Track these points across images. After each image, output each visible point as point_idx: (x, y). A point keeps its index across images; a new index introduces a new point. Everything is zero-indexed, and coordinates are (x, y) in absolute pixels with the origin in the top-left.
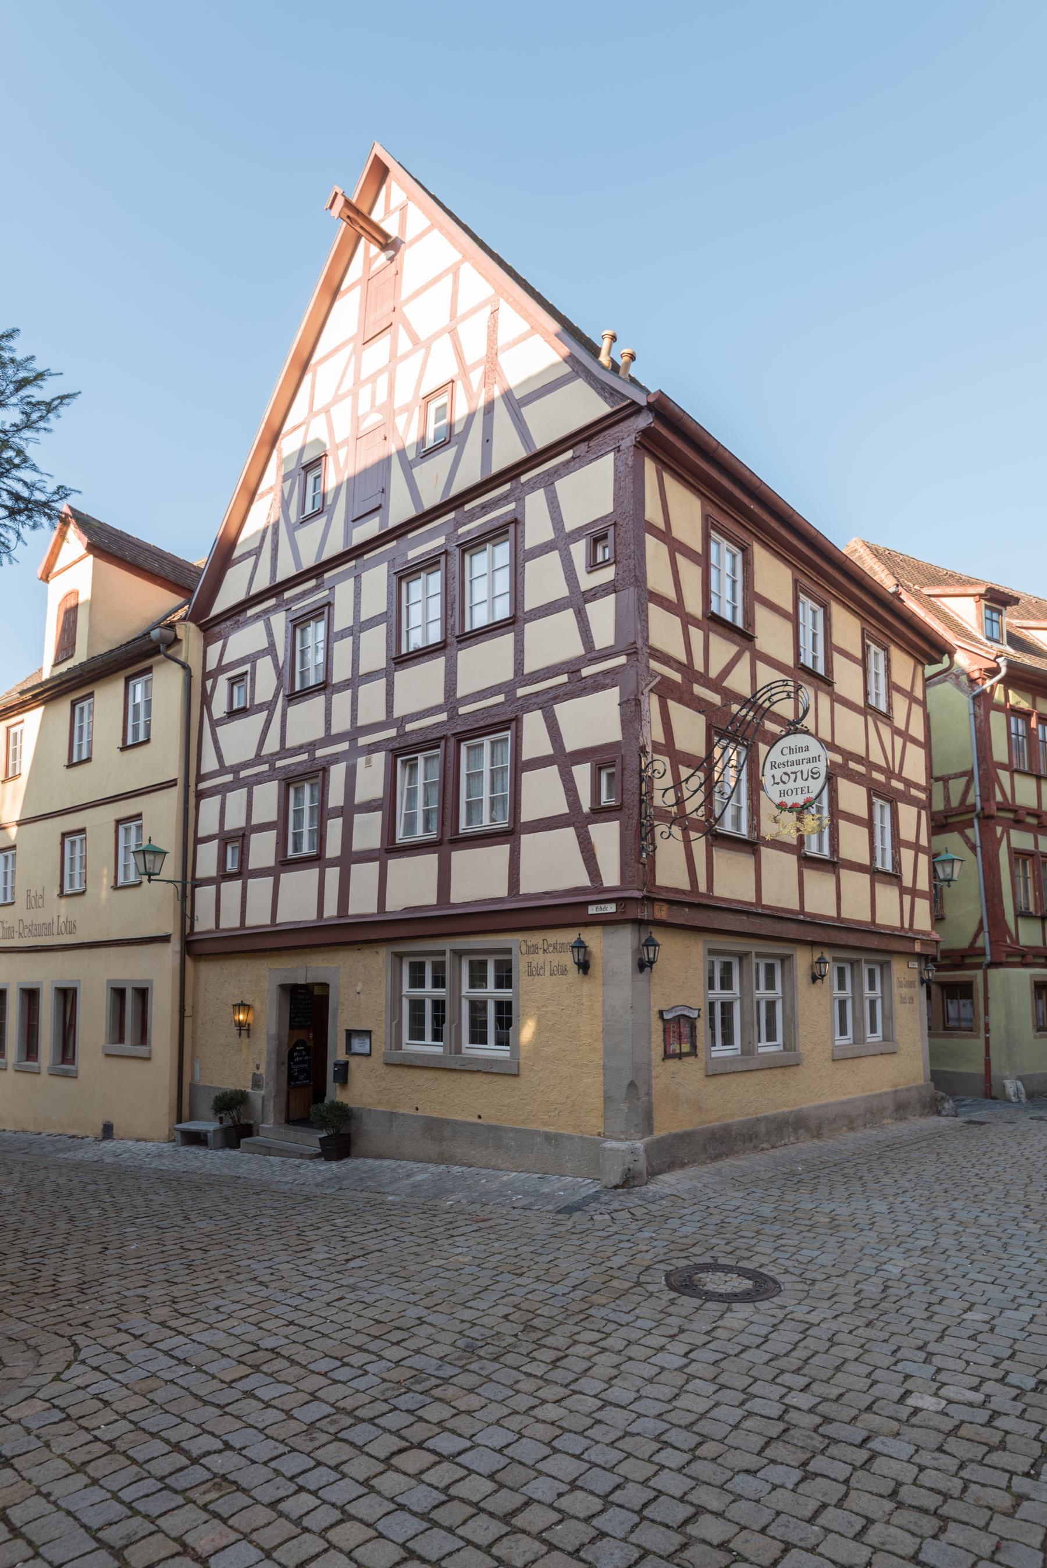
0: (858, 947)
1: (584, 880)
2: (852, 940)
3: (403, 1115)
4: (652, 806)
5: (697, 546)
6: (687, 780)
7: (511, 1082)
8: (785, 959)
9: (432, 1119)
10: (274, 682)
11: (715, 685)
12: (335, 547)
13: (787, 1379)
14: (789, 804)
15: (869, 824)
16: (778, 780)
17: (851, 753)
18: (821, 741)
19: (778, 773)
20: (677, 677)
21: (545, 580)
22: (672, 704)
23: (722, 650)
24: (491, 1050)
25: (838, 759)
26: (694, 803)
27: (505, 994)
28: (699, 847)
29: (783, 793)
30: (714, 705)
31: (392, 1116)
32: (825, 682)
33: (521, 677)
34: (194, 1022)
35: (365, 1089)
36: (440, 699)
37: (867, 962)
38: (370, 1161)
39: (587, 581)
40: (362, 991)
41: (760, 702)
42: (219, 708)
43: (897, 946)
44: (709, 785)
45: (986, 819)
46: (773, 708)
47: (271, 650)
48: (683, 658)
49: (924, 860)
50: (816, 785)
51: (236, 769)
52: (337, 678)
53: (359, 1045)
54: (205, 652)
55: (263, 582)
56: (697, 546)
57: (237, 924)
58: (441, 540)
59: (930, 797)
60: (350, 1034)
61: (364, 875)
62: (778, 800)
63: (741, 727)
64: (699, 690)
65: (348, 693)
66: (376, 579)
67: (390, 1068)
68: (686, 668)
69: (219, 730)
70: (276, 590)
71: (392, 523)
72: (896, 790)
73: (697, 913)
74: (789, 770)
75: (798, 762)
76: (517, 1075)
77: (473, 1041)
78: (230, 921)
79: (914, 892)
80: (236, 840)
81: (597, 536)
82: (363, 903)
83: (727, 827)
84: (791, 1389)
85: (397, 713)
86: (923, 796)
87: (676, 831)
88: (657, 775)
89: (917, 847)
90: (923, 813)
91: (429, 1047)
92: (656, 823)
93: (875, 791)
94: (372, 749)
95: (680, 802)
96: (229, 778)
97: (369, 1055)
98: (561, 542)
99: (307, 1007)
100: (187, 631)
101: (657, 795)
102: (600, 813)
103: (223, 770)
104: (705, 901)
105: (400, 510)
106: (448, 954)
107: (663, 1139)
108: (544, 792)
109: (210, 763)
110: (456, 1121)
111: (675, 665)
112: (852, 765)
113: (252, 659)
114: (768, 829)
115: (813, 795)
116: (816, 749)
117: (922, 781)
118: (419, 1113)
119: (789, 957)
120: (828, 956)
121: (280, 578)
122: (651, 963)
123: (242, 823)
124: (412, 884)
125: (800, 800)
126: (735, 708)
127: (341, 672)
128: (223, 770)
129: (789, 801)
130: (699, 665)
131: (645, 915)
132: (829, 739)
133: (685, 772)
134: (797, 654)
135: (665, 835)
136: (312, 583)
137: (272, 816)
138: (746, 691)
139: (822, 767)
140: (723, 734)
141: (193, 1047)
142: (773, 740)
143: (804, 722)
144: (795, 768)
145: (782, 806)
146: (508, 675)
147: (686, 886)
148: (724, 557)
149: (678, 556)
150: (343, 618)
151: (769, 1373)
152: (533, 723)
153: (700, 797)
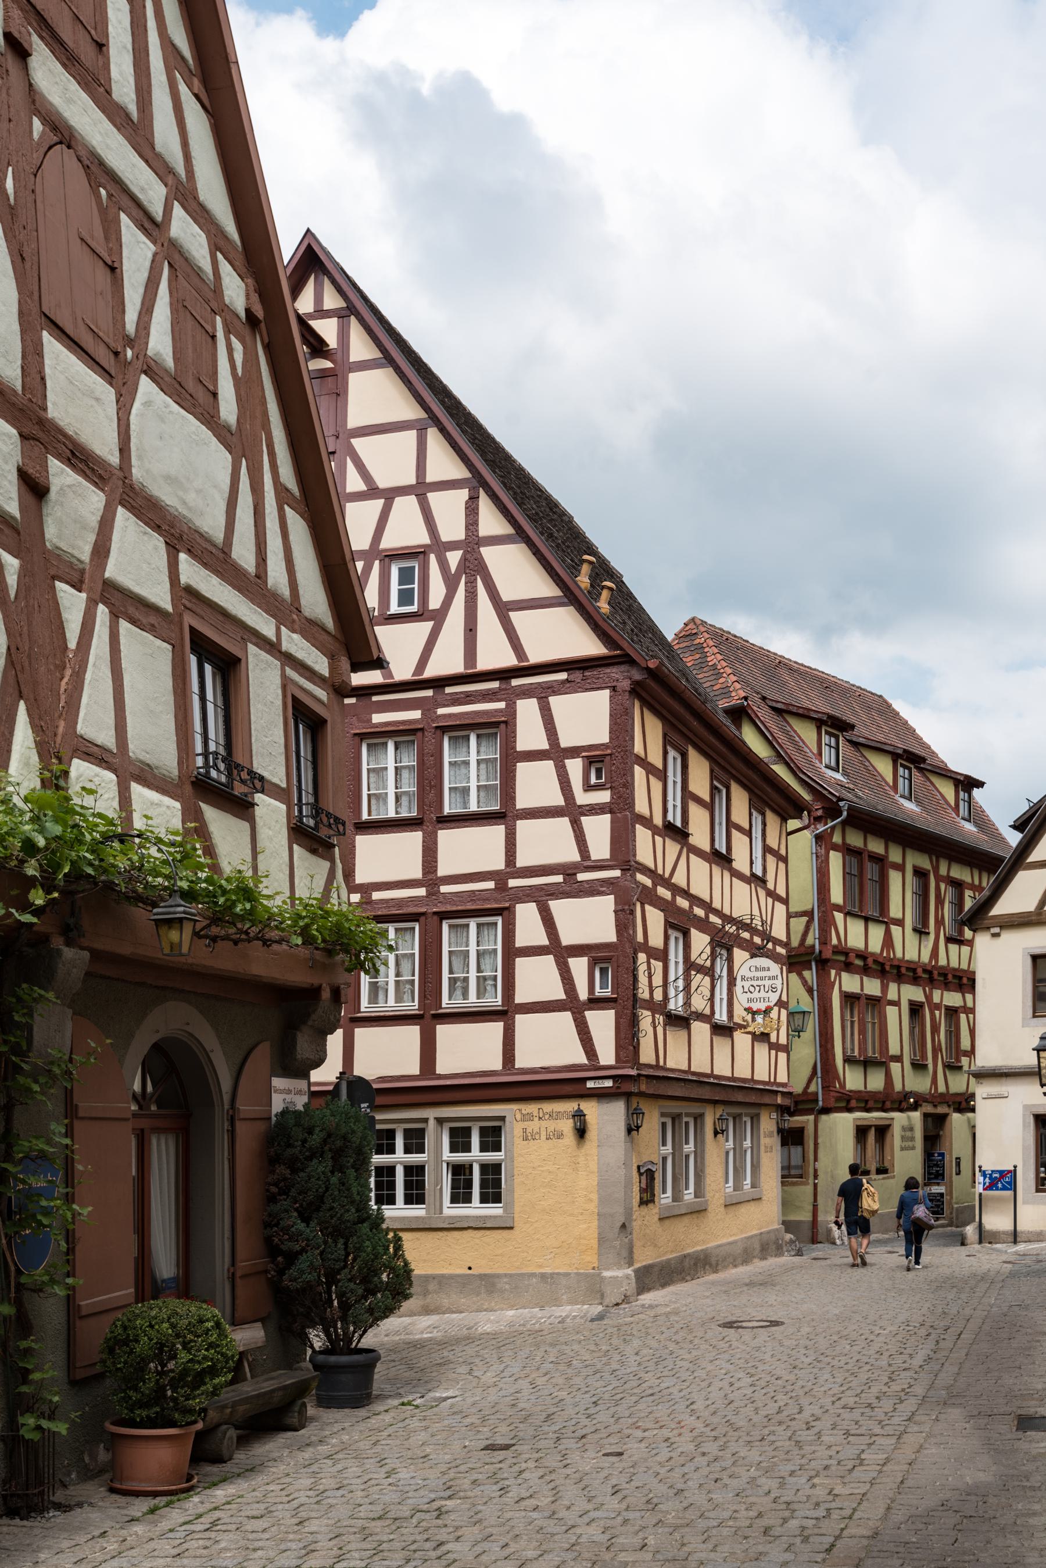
1: (582, 1059)
76: (511, 1228)
77: (455, 1199)
102: (596, 1003)
152: (527, 915)
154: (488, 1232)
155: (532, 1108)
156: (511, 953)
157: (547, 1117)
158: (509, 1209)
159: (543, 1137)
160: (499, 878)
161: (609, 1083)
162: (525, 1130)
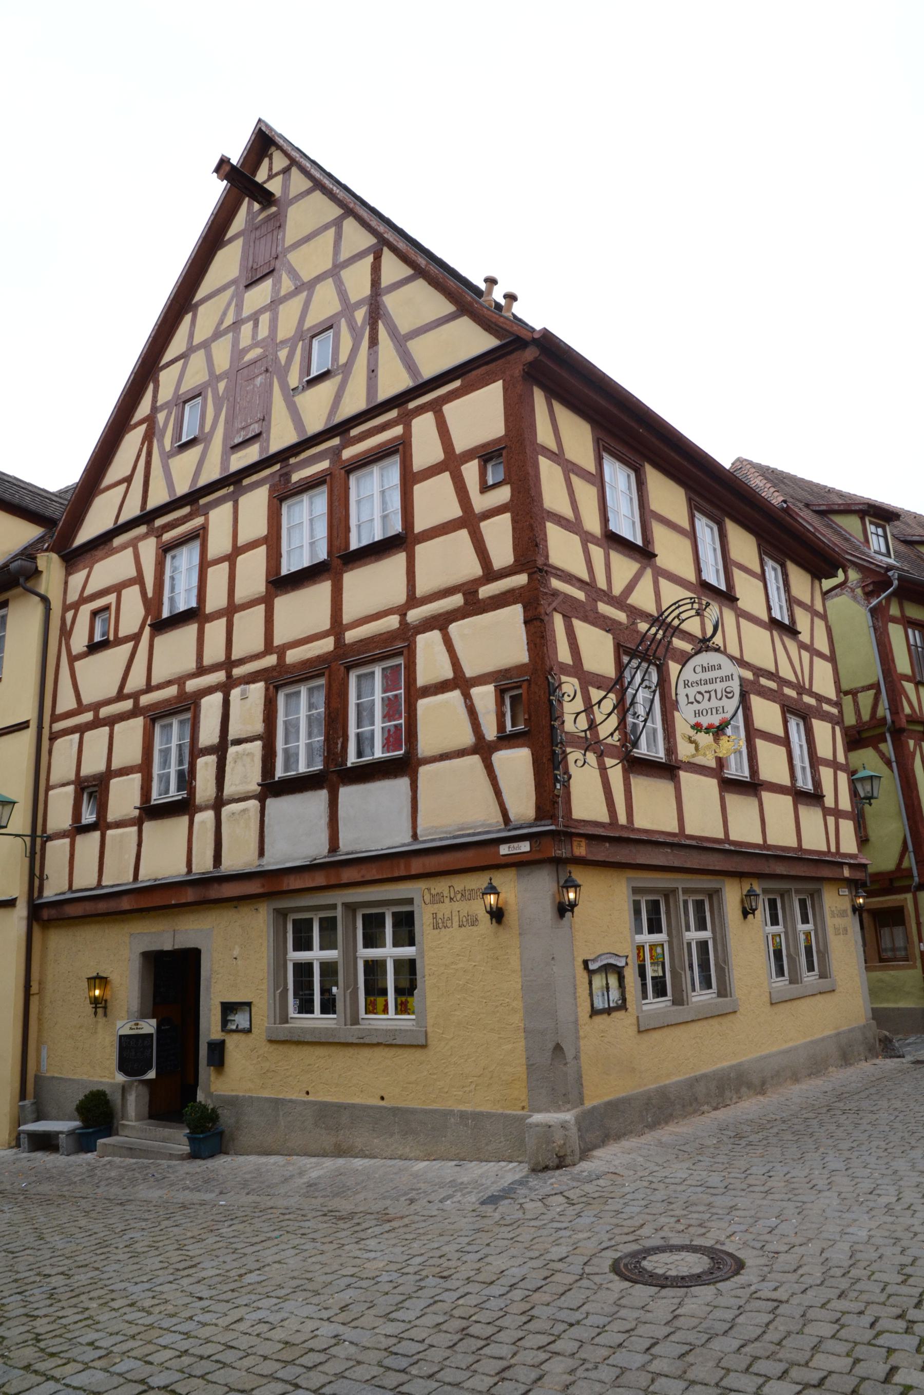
0: (783, 877)
2: (780, 869)
3: (291, 1101)
4: (563, 731)
6: (599, 703)
8: (714, 894)
10: (142, 612)
11: (619, 602)
12: (211, 474)
13: (761, 1367)
14: (705, 725)
15: (786, 742)
17: (760, 669)
18: (731, 658)
19: (691, 692)
20: (580, 595)
21: (436, 501)
22: (576, 623)
23: (624, 568)
24: (389, 1020)
25: (749, 675)
27: (407, 952)
28: (616, 774)
29: (698, 713)
30: (620, 623)
31: (277, 1103)
32: (728, 597)
33: (413, 601)
34: (41, 1001)
35: (243, 1074)
36: (326, 625)
37: (798, 891)
38: (253, 1158)
39: (480, 502)
40: (238, 959)
41: (669, 619)
43: (826, 872)
44: (623, 708)
45: (898, 734)
46: (682, 626)
47: (139, 580)
48: (585, 576)
49: (843, 777)
50: (731, 704)
51: (96, 707)
52: (210, 608)
55: (132, 510)
56: (591, 467)
57: (93, 882)
58: (325, 465)
59: (841, 712)
61: (240, 821)
62: (693, 721)
63: (648, 647)
64: (604, 608)
65: (223, 621)
66: (255, 503)
67: (275, 1046)
68: (588, 586)
69: (77, 664)
70: (147, 518)
71: (274, 448)
72: (809, 706)
73: (618, 848)
74: (703, 689)
75: (712, 681)
78: (86, 878)
79: (837, 813)
80: (93, 789)
82: (239, 856)
83: (643, 750)
84: (768, 1378)
85: (277, 642)
86: (835, 711)
87: (591, 757)
88: (566, 698)
89: (834, 764)
90: (837, 729)
91: (317, 1020)
92: (569, 750)
93: (789, 709)
94: (251, 678)
97: (249, 1031)
98: (451, 463)
99: (174, 979)
100: (49, 561)
101: (568, 719)
102: (506, 740)
105: (282, 435)
106: (339, 908)
107: (594, 1108)
108: (442, 722)
110: (353, 1106)
111: (577, 584)
112: (763, 681)
114: (684, 751)
115: (728, 716)
116: (729, 668)
117: (833, 696)
118: (311, 1098)
119: (718, 891)
120: (757, 888)
121: (151, 505)
122: (572, 905)
124: (297, 831)
125: (716, 720)
126: (643, 626)
127: (216, 600)
129: (705, 721)
130: (602, 583)
131: (562, 852)
132: (738, 655)
133: (596, 694)
134: (699, 571)
135: (580, 763)
136: (186, 510)
138: (651, 608)
139: (735, 686)
140: (633, 654)
141: (40, 1031)
142: (684, 659)
143: (714, 640)
144: (709, 687)
145: (697, 727)
146: (400, 597)
147: (605, 818)
148: (617, 476)
151: (741, 1362)
152: (429, 646)
153: (613, 721)
154: (400, 1051)
157: (459, 896)
158: (421, 1021)
159: (456, 924)
160: (402, 610)
161: (525, 847)
162: (435, 915)
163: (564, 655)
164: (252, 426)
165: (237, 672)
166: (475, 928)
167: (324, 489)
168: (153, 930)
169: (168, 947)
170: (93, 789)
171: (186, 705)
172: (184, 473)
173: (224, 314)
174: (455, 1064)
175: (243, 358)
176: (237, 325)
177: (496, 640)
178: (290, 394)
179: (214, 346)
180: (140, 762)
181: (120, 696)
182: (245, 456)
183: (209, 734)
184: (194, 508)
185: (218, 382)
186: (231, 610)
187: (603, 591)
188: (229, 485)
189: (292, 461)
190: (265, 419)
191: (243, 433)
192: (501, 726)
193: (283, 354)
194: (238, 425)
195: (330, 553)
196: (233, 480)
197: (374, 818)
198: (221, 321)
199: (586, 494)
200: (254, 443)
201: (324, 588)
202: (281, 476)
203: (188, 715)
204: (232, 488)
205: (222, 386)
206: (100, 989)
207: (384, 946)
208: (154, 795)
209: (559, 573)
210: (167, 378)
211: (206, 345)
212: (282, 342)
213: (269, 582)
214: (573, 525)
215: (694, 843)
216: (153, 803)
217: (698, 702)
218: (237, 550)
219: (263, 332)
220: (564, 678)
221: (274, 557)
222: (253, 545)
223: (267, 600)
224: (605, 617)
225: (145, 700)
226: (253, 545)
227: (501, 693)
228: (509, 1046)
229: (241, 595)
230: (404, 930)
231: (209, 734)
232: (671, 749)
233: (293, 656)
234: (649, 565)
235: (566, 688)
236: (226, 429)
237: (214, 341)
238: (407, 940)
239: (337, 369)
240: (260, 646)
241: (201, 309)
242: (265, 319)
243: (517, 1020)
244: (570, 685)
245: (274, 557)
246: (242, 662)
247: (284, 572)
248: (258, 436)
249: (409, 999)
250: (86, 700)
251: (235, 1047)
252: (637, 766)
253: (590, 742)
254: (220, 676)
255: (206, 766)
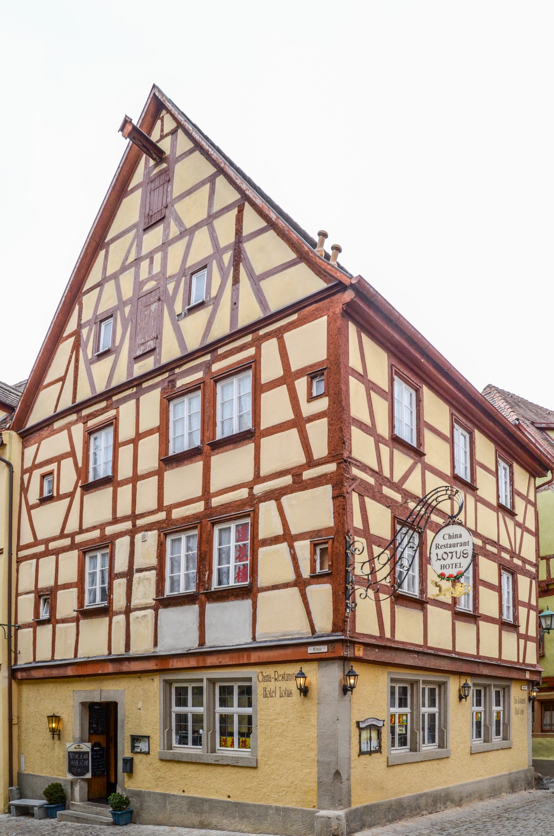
5: (385, 387)
6: (379, 556)
7: (251, 772)
9: (194, 799)
10: (75, 478)
16: (440, 557)
19: (440, 552)
20: (371, 480)
21: (276, 407)
23: (403, 461)
26: (383, 574)
27: (247, 711)
28: (386, 605)
29: (443, 567)
30: (397, 502)
33: (258, 479)
41: (430, 501)
42: (33, 496)
44: (394, 561)
47: (72, 454)
48: (376, 468)
52: (121, 476)
53: (143, 746)
54: (23, 453)
58: (199, 375)
60: (135, 739)
64: (387, 491)
66: (151, 400)
68: (377, 474)
70: (76, 408)
71: (164, 360)
73: (384, 652)
74: (448, 550)
76: (255, 768)
81: (314, 373)
82: (142, 645)
83: (405, 589)
85: (165, 504)
95: (373, 572)
96: (42, 548)
97: (148, 753)
103: (36, 543)
104: (389, 644)
105: (170, 351)
108: (274, 564)
109: (27, 538)
111: (370, 473)
113: (58, 459)
114: (432, 592)
121: (79, 400)
123: (52, 583)
126: (412, 505)
127: (125, 472)
128: (36, 543)
130: (386, 473)
133: (377, 550)
135: (363, 596)
136: (104, 404)
137: (74, 578)
138: (418, 492)
140: (404, 524)
146: (250, 476)
147: (377, 634)
149: (372, 393)
150: (126, 431)
152: (268, 513)
153: (387, 569)
155: (269, 671)
156: (257, 543)
160: (250, 486)
161: (324, 649)
163: (358, 523)
164: (149, 343)
165: (140, 522)
166: (290, 698)
167: (199, 393)
168: (88, 689)
169: (97, 700)
170: (46, 596)
171: (106, 544)
172: (101, 375)
173: (129, 252)
174: (274, 779)
175: (142, 288)
176: (138, 260)
177: (312, 510)
178: (176, 318)
179: (121, 277)
180: (76, 581)
181: (62, 535)
182: (144, 365)
183: (121, 565)
184: (109, 402)
185: (124, 306)
186: (135, 479)
187: (387, 478)
188: (133, 387)
189: (177, 371)
190: (157, 338)
191: (142, 348)
192: (313, 569)
193: (171, 287)
194: (139, 341)
195: (202, 441)
196: (136, 383)
197: (229, 625)
198: (126, 258)
199: (381, 406)
200: (150, 356)
201: (198, 466)
202: (169, 382)
203: (108, 551)
204: (135, 390)
205: (127, 309)
206: (55, 723)
207: (232, 706)
208: (86, 603)
209: (358, 464)
210: (88, 301)
211: (115, 276)
212: (170, 277)
213: (160, 460)
214: (369, 430)
215: (432, 652)
216: (85, 608)
217: (444, 559)
218: (139, 436)
219: (157, 268)
220: (356, 538)
221: (164, 442)
222: (150, 433)
223: (159, 473)
224: (387, 497)
225: (79, 539)
226: (150, 433)
227: (315, 545)
228: (308, 771)
229: (142, 469)
230: (245, 697)
231: (121, 565)
232: (423, 591)
233: (177, 514)
234: (419, 461)
235: (357, 545)
236: (130, 344)
237: (121, 274)
238: (247, 703)
239: (210, 301)
240: (155, 506)
241: (112, 247)
242: (158, 257)
243: (313, 755)
244: (360, 543)
245: (164, 442)
246: (142, 515)
247: (171, 453)
248: (154, 350)
249: (247, 739)
250: (40, 537)
251: (141, 764)
252: (400, 599)
253: (371, 583)
254: (127, 525)
255: (120, 585)
